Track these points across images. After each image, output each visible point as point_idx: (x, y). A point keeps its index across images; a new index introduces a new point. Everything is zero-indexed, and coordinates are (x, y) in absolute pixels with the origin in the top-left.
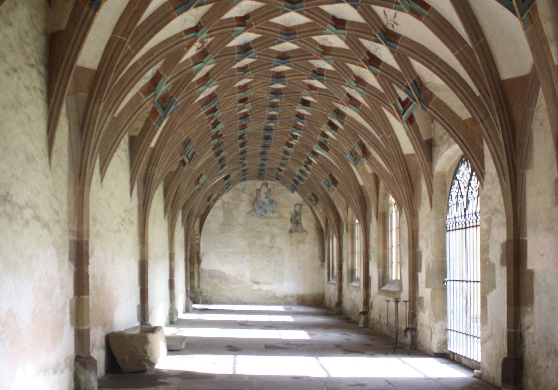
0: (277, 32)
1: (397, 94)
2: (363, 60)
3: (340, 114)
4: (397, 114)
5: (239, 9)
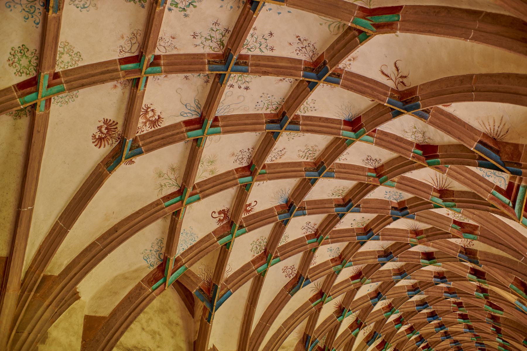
4: (503, 209)
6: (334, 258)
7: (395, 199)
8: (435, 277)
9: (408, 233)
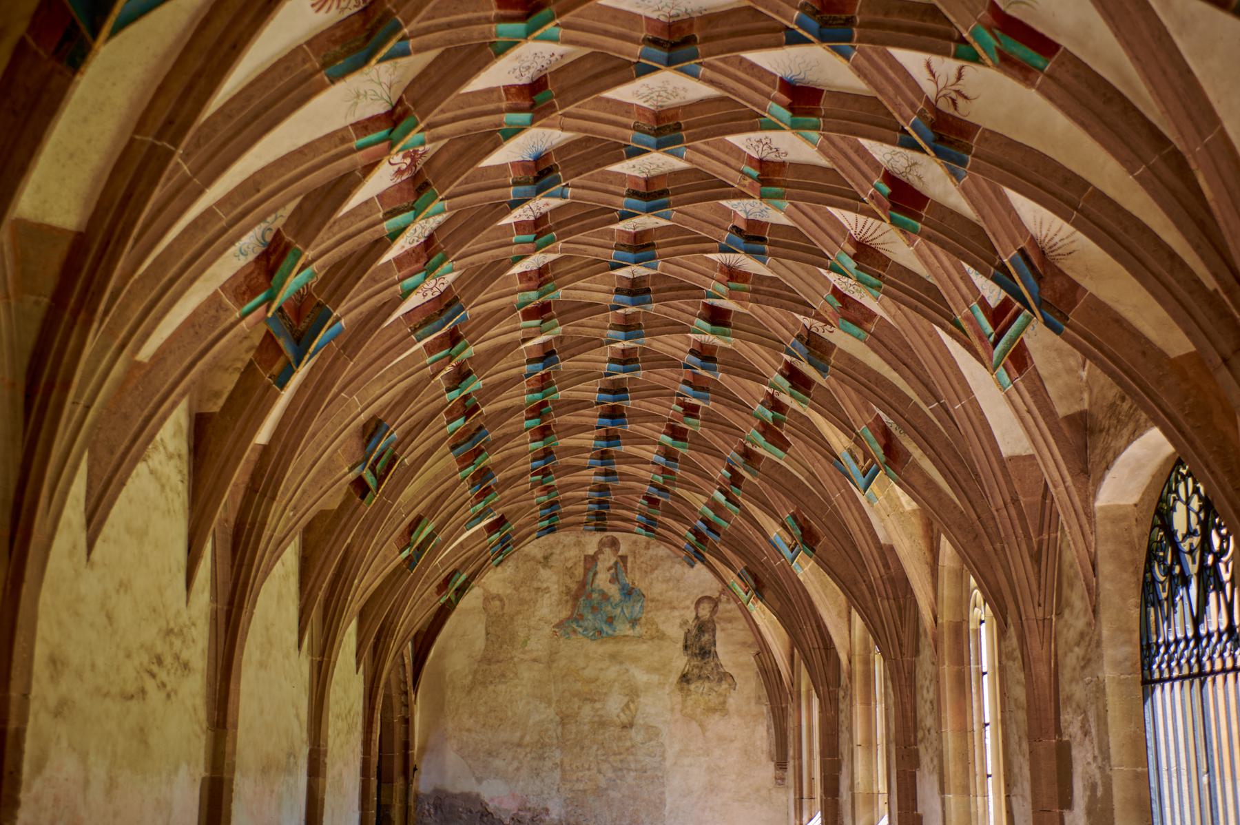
0: (626, 126)
1: (974, 289)
2: (872, 197)
3: (816, 347)
5: (516, 64)
7: (745, 212)
8: (692, 352)
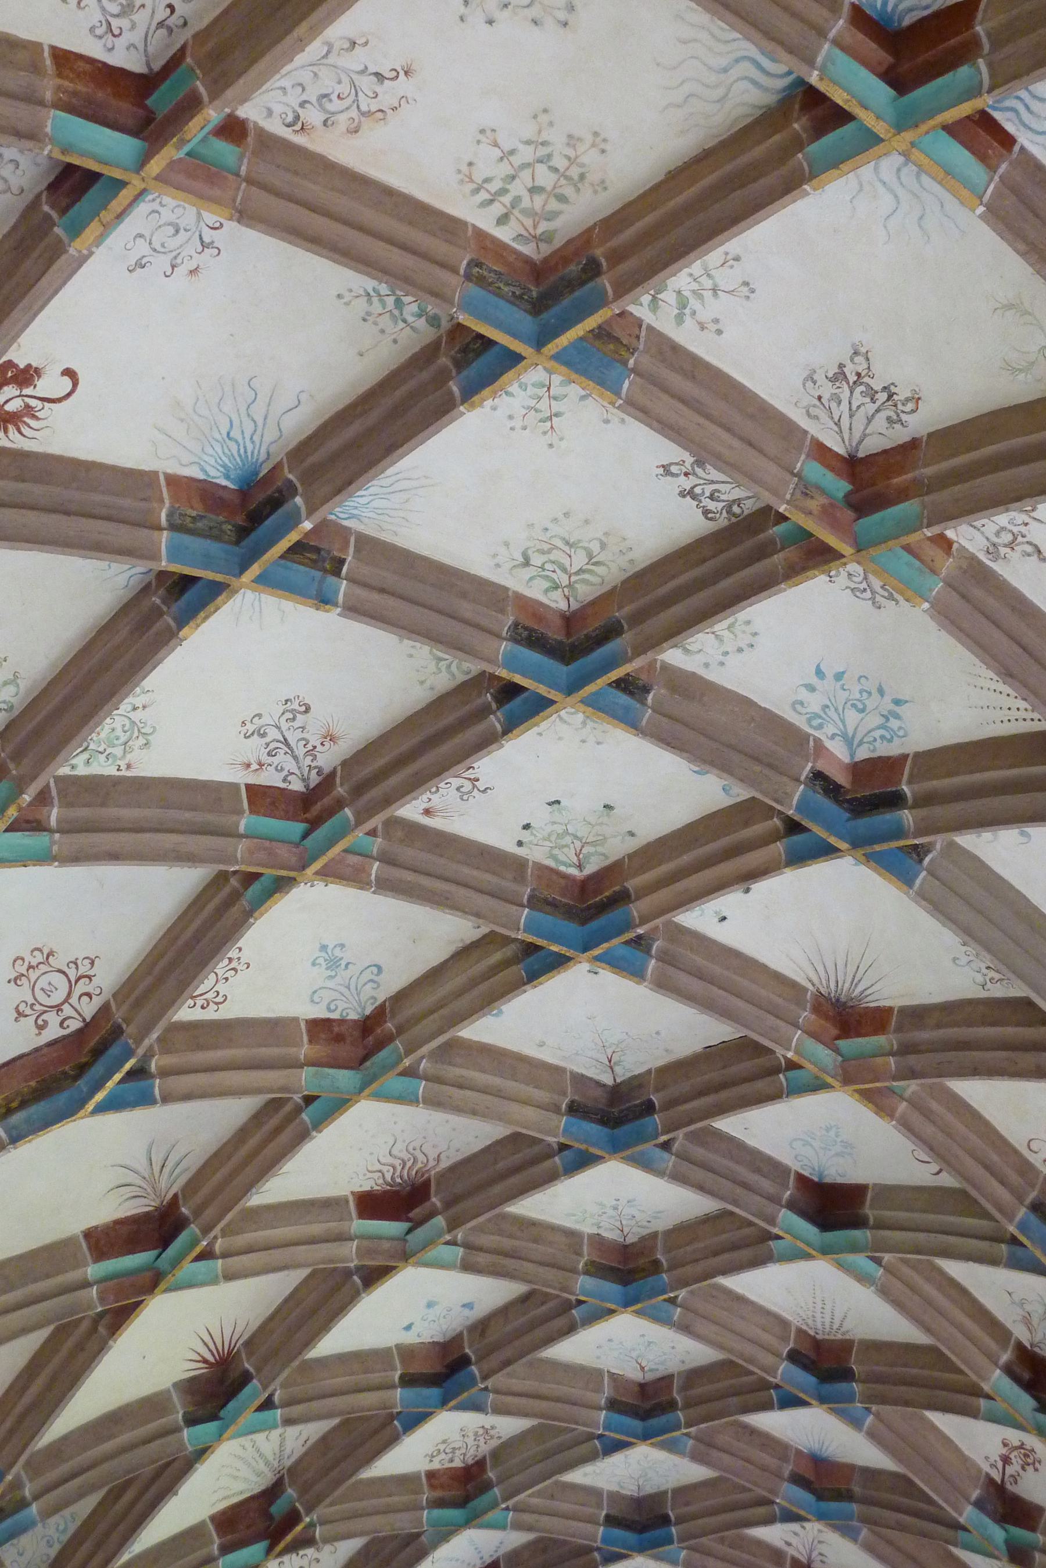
6: (328, 1020)
7: (844, 736)
8: (794, 1357)
9: (800, 1003)
